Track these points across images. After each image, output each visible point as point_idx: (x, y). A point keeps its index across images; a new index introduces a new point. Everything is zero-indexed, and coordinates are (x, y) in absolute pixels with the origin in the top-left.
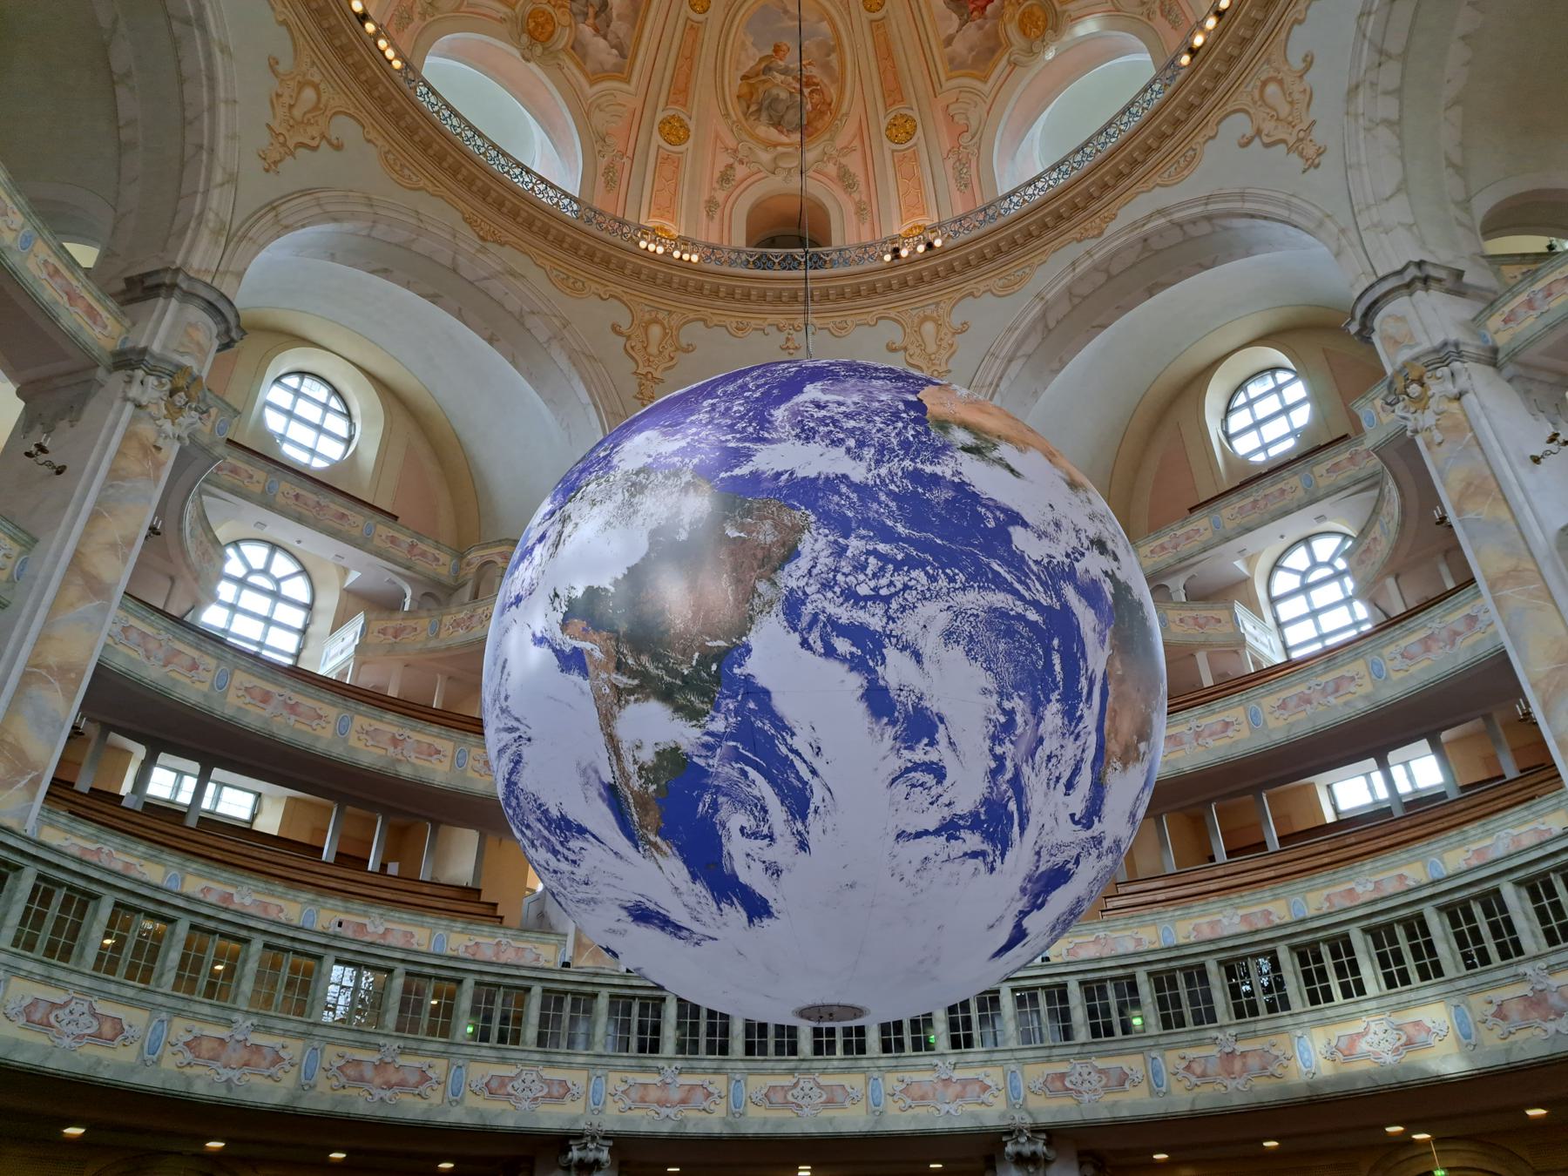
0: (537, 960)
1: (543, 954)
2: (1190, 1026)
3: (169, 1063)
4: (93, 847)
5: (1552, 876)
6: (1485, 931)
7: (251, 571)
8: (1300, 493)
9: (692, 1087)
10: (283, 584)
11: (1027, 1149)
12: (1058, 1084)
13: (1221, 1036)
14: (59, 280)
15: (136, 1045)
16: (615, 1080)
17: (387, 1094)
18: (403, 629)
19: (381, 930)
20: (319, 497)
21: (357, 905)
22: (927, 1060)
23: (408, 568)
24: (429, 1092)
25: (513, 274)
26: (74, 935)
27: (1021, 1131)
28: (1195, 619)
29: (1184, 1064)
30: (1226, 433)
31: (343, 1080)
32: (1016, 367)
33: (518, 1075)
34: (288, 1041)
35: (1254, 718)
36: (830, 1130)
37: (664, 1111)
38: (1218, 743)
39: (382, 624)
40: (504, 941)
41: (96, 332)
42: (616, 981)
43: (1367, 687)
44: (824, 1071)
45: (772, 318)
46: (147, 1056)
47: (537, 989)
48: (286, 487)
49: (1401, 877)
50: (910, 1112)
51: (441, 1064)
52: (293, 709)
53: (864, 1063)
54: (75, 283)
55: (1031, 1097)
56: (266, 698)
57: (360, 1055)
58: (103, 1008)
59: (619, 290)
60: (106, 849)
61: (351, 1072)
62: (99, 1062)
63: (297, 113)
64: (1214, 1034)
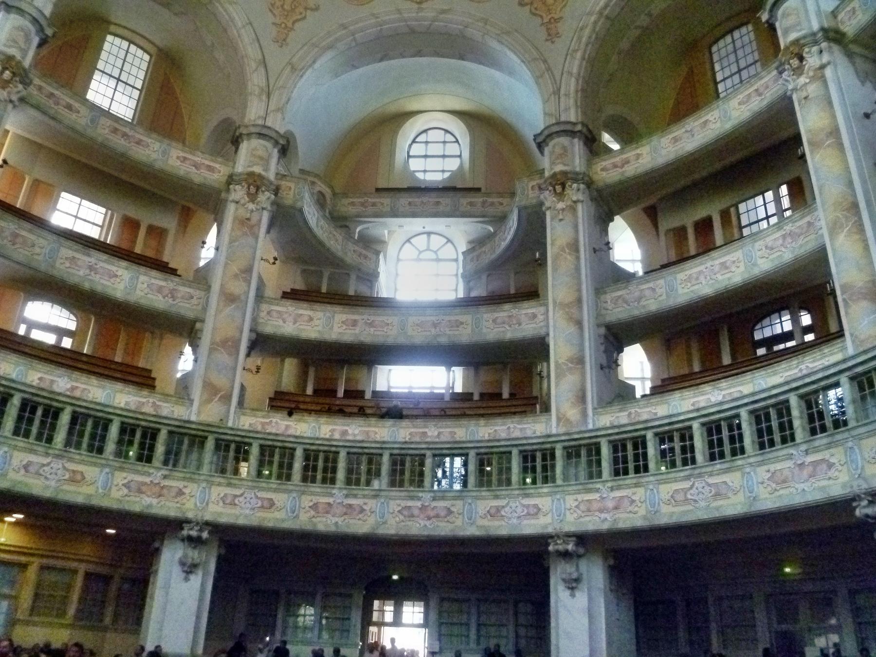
0: (534, 433)
7: (420, 252)
14: (188, 162)
16: (571, 501)
17: (428, 523)
19: (436, 433)
23: (483, 216)
25: (444, 12)
31: (402, 517)
33: (508, 504)
34: (366, 501)
37: (603, 516)
41: (216, 176)
44: (711, 474)
47: (515, 452)
50: (777, 494)
54: (196, 159)
55: (867, 466)
56: (355, 323)
57: (410, 503)
60: (274, 420)
61: (406, 513)
62: (264, 519)
63: (285, 7)
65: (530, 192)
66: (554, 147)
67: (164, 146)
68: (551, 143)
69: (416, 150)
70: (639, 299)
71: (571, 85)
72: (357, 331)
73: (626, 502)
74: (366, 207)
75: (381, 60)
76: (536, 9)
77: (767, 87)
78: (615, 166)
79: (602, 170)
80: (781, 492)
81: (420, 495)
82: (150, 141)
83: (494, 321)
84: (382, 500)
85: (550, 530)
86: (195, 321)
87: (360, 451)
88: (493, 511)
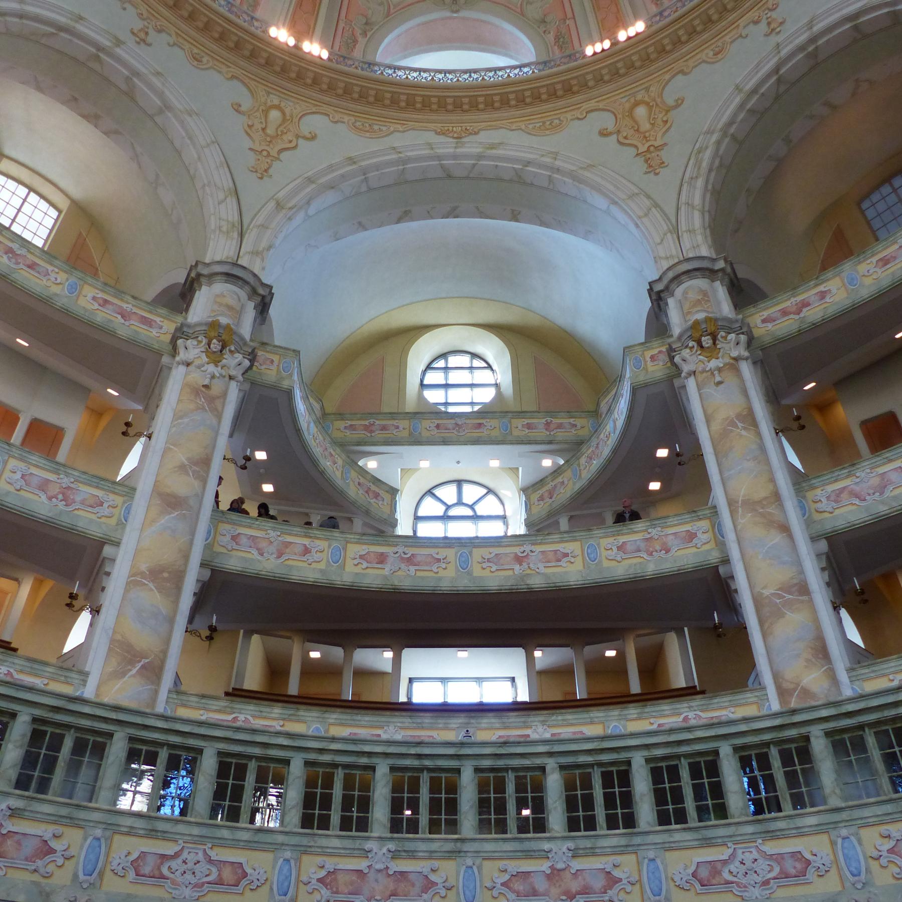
4: (230, 717)
7: (448, 507)
10: (477, 508)
14: (110, 307)
23: (550, 442)
25: (492, 147)
33: (733, 856)
34: (436, 864)
45: (742, 22)
51: (628, 861)
54: (125, 306)
56: (382, 559)
59: (592, 104)
61: (519, 886)
63: (269, 131)
65: (649, 364)
66: (685, 293)
67: (73, 279)
68: (679, 291)
69: (432, 378)
70: (882, 489)
72: (386, 572)
74: (371, 432)
75: (399, 221)
76: (625, 138)
78: (785, 313)
79: (764, 321)
81: (546, 846)
82: (50, 268)
83: (619, 548)
84: (469, 862)
86: (101, 544)
87: (416, 763)
88: (704, 873)
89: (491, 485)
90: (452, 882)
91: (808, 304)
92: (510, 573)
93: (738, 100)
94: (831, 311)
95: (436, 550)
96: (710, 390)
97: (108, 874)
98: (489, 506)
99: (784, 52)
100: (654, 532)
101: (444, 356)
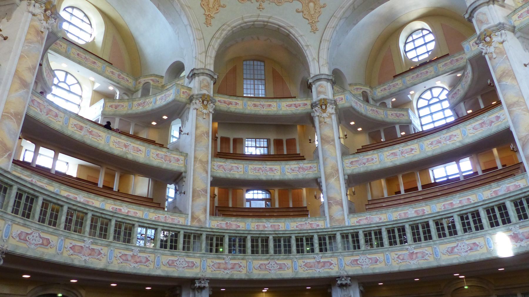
1: (179, 220)
2: (398, 244)
3: (65, 254)
5: (523, 199)
6: (498, 215)
7: (60, 82)
8: (433, 73)
9: (235, 264)
10: (71, 87)
11: (344, 282)
12: (355, 263)
13: (409, 248)
15: (55, 248)
17: (136, 265)
18: (119, 106)
20: (84, 54)
21: (118, 202)
22: (312, 256)
23: (118, 83)
24: (149, 265)
26: (30, 210)
27: (343, 277)
28: (396, 114)
29: (397, 256)
30: (405, 50)
31: (121, 260)
32: (342, 21)
34: (102, 248)
35: (421, 148)
36: (280, 277)
37: (226, 271)
38: (409, 156)
39: (112, 104)
40: (167, 216)
42: (208, 230)
43: (460, 139)
44: (278, 259)
46: (58, 252)
48: (74, 51)
49: (468, 199)
50: (307, 271)
52: (90, 133)
53: (292, 257)
55: (346, 266)
56: (81, 128)
58: (43, 235)
61: (124, 258)
62: (43, 253)
64: (407, 247)
65: (182, 94)
66: (203, 80)
68: (202, 77)
70: (231, 170)
71: (213, 53)
73: (237, 266)
77: (300, 106)
78: (225, 102)
80: (309, 271)
83: (157, 155)
85: (199, 276)
89: (80, 81)
90: (106, 254)
91: (232, 104)
92: (121, 150)
93: (240, 22)
94: (237, 111)
95: (100, 132)
96: (200, 118)
97: (11, 237)
98: (75, 89)
99: (260, 19)
100: (168, 154)
101: (73, 7)
